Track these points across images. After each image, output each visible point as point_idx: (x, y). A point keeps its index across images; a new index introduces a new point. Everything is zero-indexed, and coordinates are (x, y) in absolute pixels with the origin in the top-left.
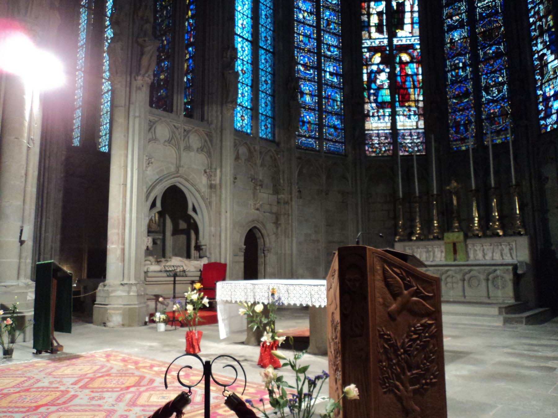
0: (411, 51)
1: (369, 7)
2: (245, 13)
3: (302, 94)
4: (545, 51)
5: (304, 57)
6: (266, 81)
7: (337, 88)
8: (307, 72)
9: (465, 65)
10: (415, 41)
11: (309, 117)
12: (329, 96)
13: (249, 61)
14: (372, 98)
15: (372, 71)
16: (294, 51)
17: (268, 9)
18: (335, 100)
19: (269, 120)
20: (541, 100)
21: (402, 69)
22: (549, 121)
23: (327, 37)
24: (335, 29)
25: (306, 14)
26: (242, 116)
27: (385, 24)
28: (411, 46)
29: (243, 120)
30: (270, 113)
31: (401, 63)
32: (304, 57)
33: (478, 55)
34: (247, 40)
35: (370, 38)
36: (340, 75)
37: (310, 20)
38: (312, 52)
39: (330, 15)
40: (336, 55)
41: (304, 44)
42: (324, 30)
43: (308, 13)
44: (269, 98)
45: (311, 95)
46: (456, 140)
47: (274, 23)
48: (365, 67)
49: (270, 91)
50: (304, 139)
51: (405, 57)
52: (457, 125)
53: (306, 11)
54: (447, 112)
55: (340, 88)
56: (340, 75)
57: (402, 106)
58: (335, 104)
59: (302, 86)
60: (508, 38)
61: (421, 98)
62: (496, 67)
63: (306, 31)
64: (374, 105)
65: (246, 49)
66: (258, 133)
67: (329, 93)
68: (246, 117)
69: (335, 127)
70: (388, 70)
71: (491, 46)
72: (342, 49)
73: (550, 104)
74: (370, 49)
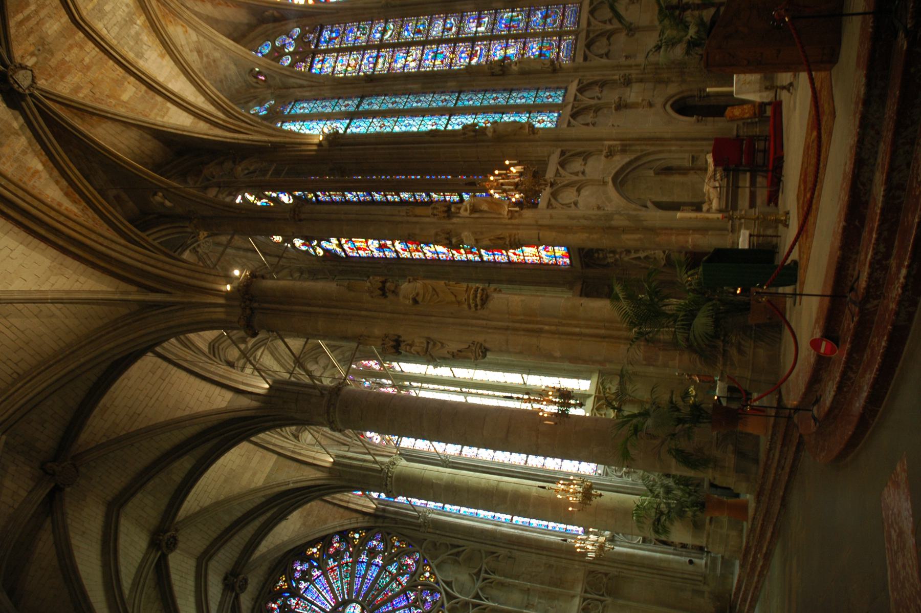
2: (419, 123)
3: (506, 57)
5: (461, 58)
6: (494, 99)
7: (495, 17)
8: (478, 53)
11: (534, 48)
12: (506, 26)
13: (474, 116)
16: (454, 70)
17: (409, 100)
18: (512, 18)
19: (541, 93)
23: (434, 33)
24: (423, 24)
25: (410, 59)
26: (539, 122)
29: (544, 121)
30: (532, 94)
32: (461, 58)
34: (449, 120)
36: (480, 13)
37: (416, 54)
38: (454, 49)
39: (408, 30)
40: (454, 20)
41: (445, 59)
42: (427, 37)
43: (407, 56)
44: (514, 95)
45: (507, 47)
47: (424, 93)
49: (505, 94)
50: (561, 54)
53: (406, 59)
55: (496, 13)
56: (480, 13)
58: (516, 18)
59: (496, 59)
63: (430, 57)
65: (459, 120)
66: (557, 105)
67: (503, 26)
68: (540, 118)
69: (545, 17)
72: (447, 14)
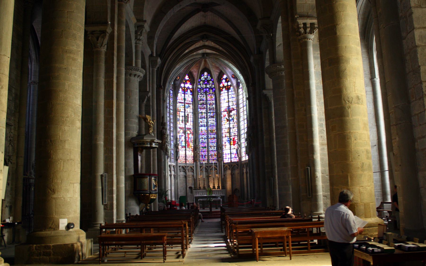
0: (190, 130)
1: (179, 114)
4: (226, 142)
9: (205, 138)
10: (191, 127)
14: (180, 144)
15: (180, 136)
20: (224, 153)
21: (188, 136)
22: (226, 160)
27: (184, 120)
28: (190, 129)
31: (188, 134)
33: (209, 136)
35: (180, 124)
46: (202, 160)
48: (178, 134)
51: (189, 132)
52: (202, 156)
54: (200, 151)
57: (188, 148)
60: (217, 134)
61: (193, 146)
62: (213, 141)
64: (181, 146)
70: (184, 136)
71: (213, 134)
73: (227, 156)
74: (180, 128)
